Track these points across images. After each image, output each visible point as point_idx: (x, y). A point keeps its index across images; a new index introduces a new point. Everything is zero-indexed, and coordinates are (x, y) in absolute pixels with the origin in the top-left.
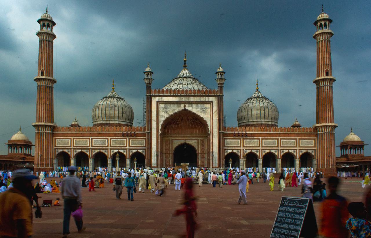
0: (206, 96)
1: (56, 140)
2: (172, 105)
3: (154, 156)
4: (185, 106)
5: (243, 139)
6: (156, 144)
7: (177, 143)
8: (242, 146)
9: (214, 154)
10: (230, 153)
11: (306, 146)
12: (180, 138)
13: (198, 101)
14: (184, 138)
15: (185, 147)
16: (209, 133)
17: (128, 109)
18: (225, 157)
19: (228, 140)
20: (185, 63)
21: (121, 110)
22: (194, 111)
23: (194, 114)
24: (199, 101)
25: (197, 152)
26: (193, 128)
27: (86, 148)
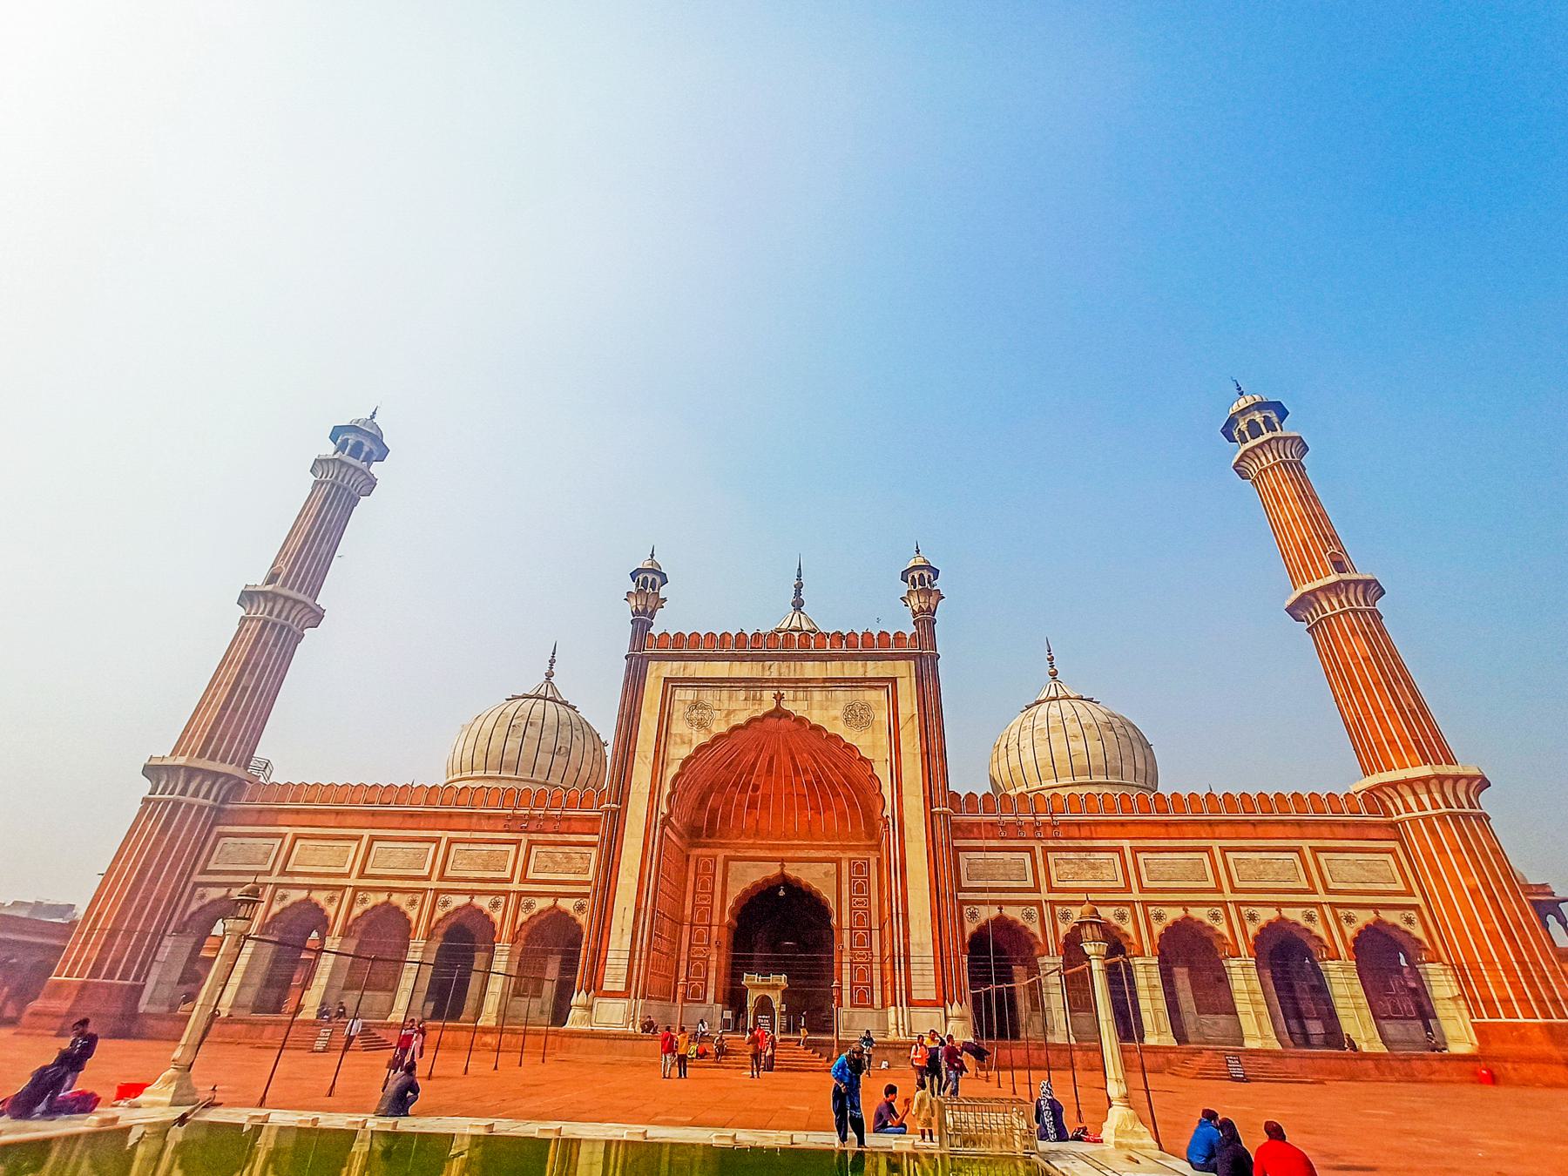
0: (867, 658)
1: (223, 841)
2: (725, 694)
5: (1046, 850)
7: (748, 876)
8: (1044, 887)
11: (1361, 887)
12: (762, 854)
18: (970, 944)
19: (972, 855)
21: (549, 738)
22: (816, 718)
23: (818, 729)
25: (834, 921)
26: (816, 809)
27: (332, 881)
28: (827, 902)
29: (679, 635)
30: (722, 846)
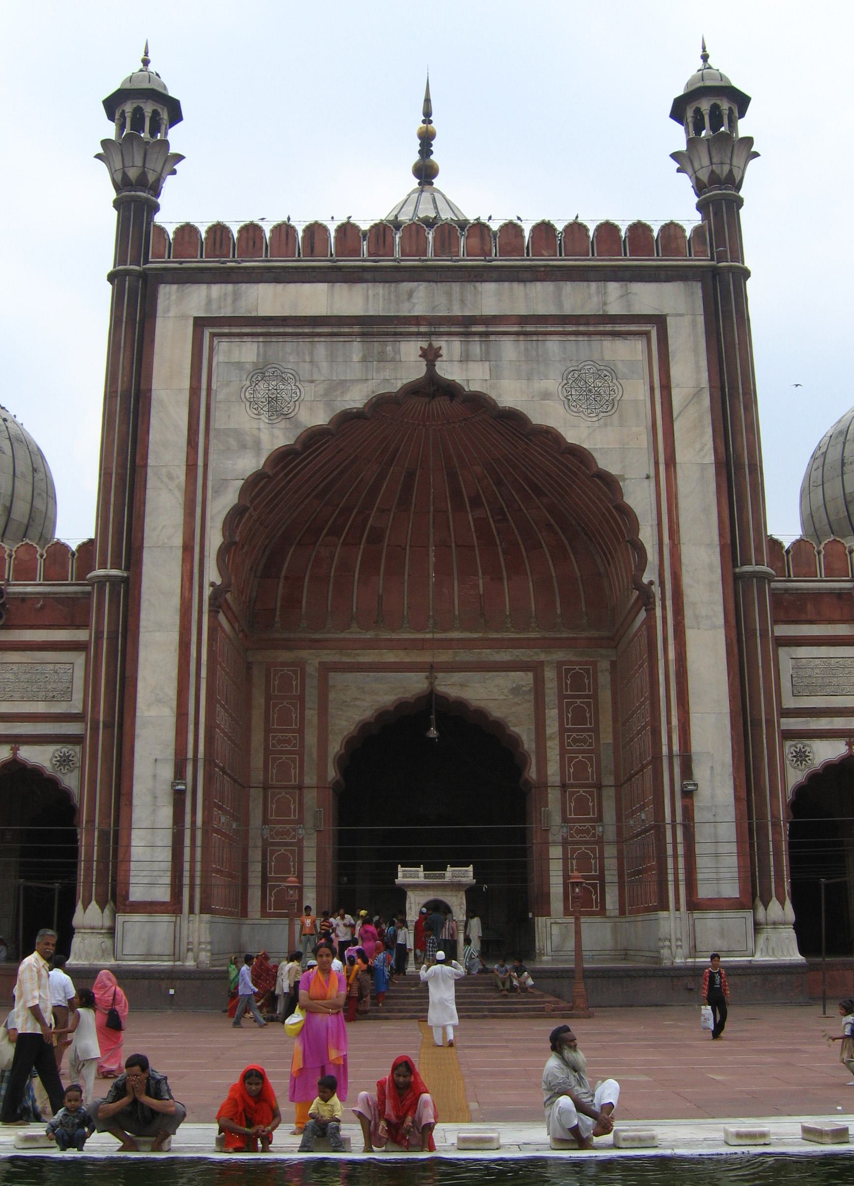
2: (321, 349)
3: (155, 797)
4: (431, 356)
6: (171, 691)
9: (701, 773)
10: (830, 768)
12: (390, 657)
13: (541, 310)
14: (426, 657)
15: (433, 733)
16: (645, 580)
17: (8, 451)
19: (803, 652)
20: (426, 149)
24: (552, 311)
25: (532, 773)
28: (515, 741)
29: (219, 231)
30: (316, 644)
